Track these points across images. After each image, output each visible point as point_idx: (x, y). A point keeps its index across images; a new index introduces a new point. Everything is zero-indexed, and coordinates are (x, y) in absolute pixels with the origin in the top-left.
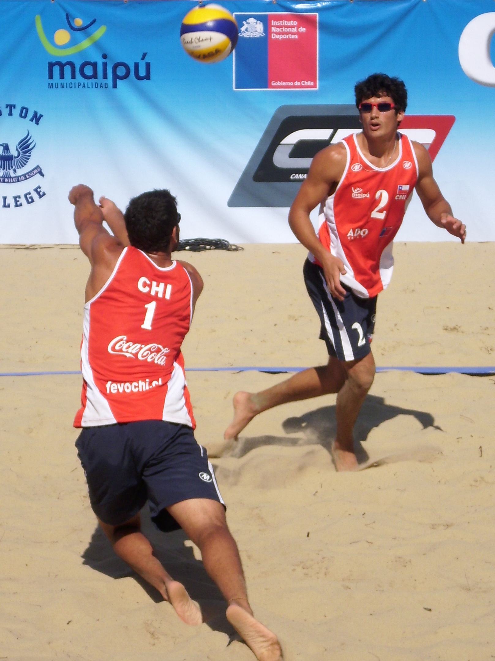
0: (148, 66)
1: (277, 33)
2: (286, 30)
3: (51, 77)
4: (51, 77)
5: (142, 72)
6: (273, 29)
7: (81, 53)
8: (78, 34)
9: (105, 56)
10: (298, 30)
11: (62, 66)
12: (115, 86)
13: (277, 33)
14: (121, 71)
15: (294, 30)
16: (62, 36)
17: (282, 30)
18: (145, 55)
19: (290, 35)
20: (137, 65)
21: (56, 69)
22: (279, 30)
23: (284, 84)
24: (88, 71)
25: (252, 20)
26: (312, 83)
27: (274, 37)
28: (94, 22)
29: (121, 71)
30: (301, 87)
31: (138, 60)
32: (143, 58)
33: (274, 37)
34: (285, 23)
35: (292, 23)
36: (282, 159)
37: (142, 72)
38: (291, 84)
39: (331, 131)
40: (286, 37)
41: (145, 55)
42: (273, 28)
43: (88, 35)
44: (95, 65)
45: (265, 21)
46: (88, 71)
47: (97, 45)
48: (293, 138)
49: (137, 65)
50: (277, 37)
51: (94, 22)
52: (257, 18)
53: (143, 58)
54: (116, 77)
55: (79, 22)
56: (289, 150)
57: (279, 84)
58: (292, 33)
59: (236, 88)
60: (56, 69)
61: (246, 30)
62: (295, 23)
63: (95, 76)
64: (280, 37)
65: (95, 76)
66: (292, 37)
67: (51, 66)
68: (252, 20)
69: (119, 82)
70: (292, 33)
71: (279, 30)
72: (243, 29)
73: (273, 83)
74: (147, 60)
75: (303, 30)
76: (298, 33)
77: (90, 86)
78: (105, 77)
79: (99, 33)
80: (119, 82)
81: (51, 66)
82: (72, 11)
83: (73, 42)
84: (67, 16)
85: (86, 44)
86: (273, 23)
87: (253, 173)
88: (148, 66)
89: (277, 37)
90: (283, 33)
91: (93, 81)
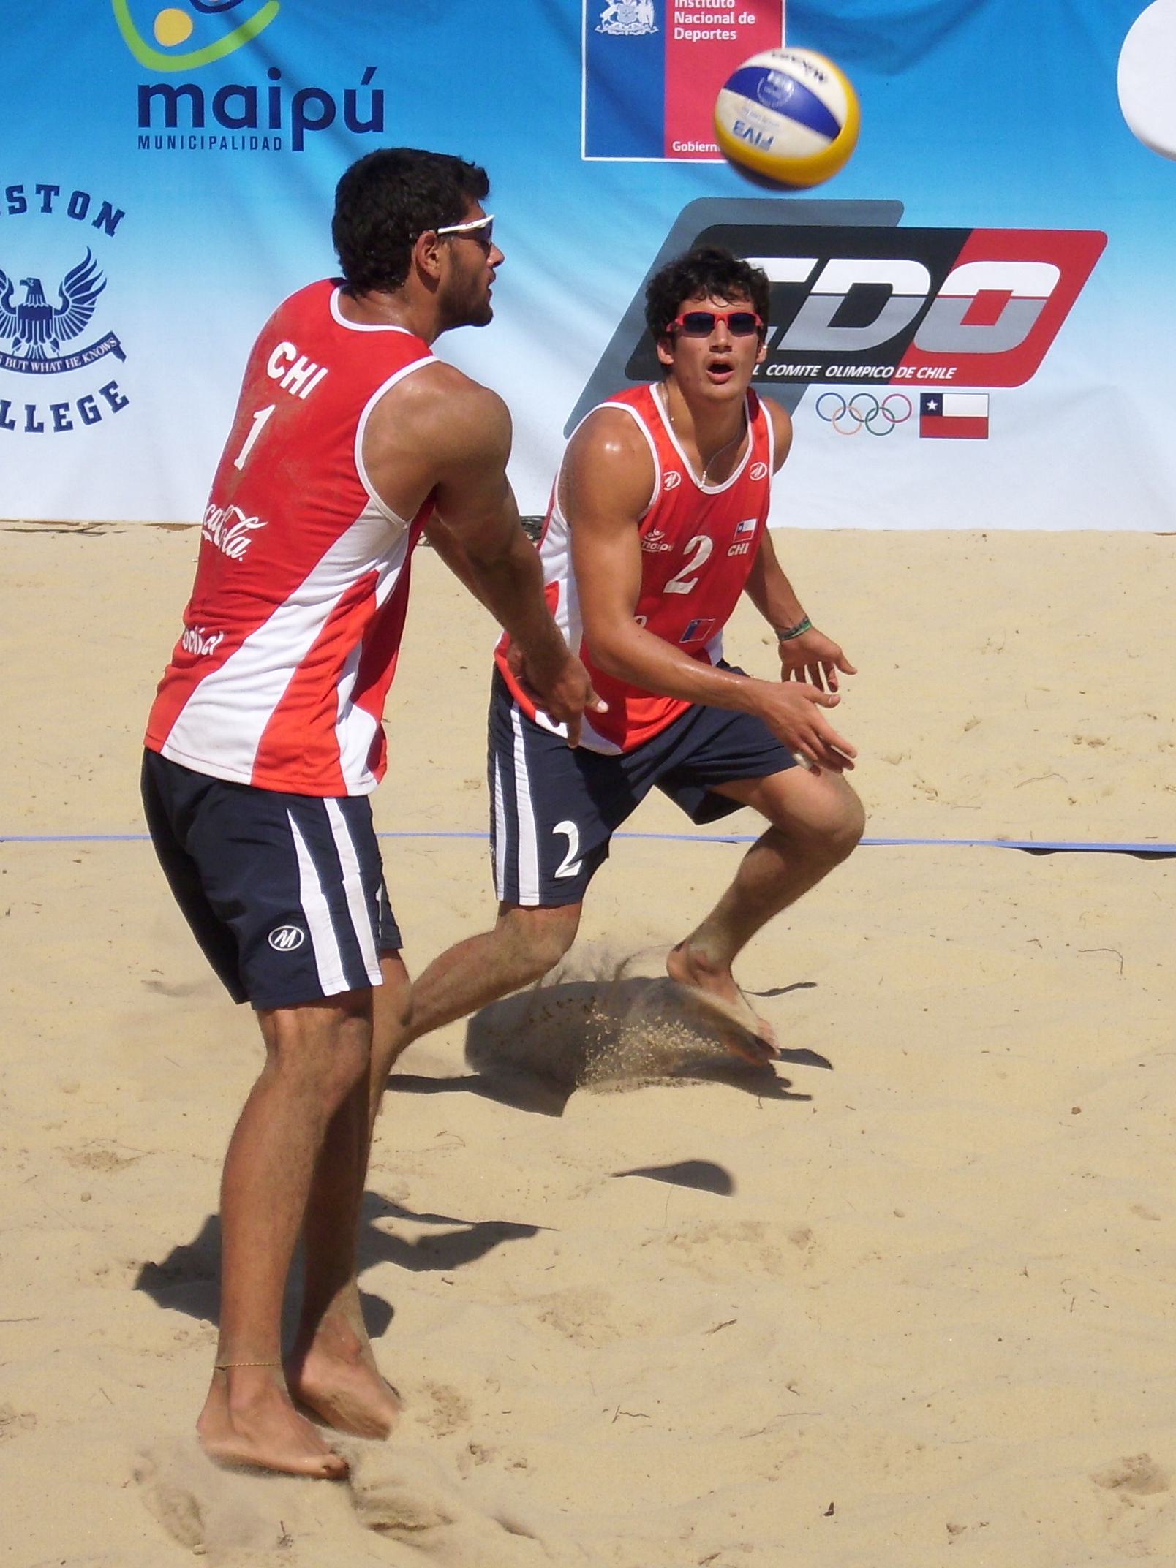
0: (378, 97)
1: (686, 27)
3: (145, 120)
4: (145, 120)
7: (219, 65)
9: (275, 73)
10: (736, 18)
11: (171, 95)
12: (298, 145)
13: (686, 27)
14: (314, 110)
15: (728, 19)
16: (174, 25)
17: (699, 19)
18: (370, 72)
19: (718, 32)
20: (351, 96)
21: (158, 102)
22: (691, 19)
24: (236, 107)
27: (680, 34)
29: (314, 110)
31: (355, 84)
32: (366, 81)
33: (680, 34)
40: (708, 35)
41: (370, 72)
42: (677, 14)
43: (236, 23)
44: (250, 94)
46: (236, 107)
47: (256, 45)
49: (351, 96)
53: (366, 81)
54: (301, 123)
57: (690, 147)
59: (587, 155)
60: (158, 102)
61: (614, 17)
63: (250, 120)
64: (696, 36)
65: (250, 120)
66: (725, 35)
67: (146, 94)
71: (691, 19)
72: (606, 15)
73: (678, 146)
74: (376, 83)
76: (735, 26)
77: (239, 143)
78: (275, 122)
81: (146, 94)
83: (198, 40)
85: (229, 44)
88: (378, 97)
91: (245, 131)
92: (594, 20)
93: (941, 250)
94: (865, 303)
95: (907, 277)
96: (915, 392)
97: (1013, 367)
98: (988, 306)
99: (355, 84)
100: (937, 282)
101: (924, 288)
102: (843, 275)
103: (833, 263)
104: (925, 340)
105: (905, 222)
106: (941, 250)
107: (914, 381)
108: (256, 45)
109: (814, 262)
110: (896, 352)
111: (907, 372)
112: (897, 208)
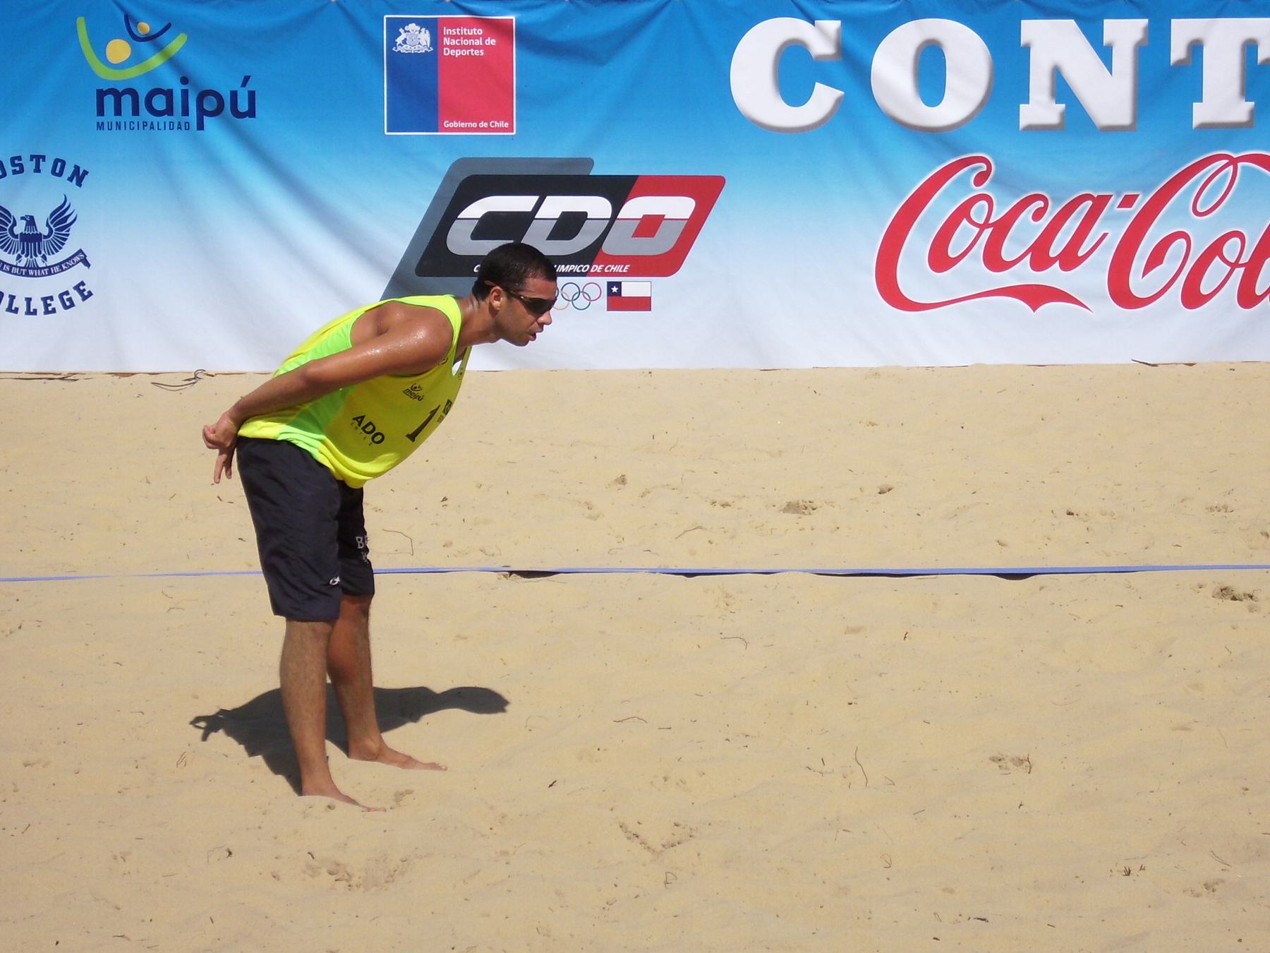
0: (252, 95)
1: (451, 47)
2: (465, 42)
3: (101, 112)
4: (101, 112)
5: (243, 106)
6: (446, 41)
7: (150, 75)
8: (144, 46)
9: (184, 80)
11: (117, 95)
12: (201, 126)
13: (451, 47)
14: (210, 104)
15: (478, 42)
16: (119, 50)
18: (246, 79)
20: (234, 95)
21: (109, 101)
22: (454, 42)
23: (462, 125)
24: (159, 103)
25: (412, 27)
26: (506, 125)
28: (169, 26)
29: (210, 104)
30: (489, 129)
31: (237, 86)
32: (244, 85)
33: (447, 52)
34: (465, 31)
35: (474, 31)
36: (461, 241)
37: (243, 106)
38: (474, 125)
39: (534, 199)
40: (465, 53)
41: (246, 79)
43: (160, 48)
44: (169, 94)
45: (434, 28)
46: (159, 103)
47: (173, 62)
48: (476, 210)
49: (234, 95)
50: (452, 52)
51: (169, 26)
52: (421, 23)
53: (244, 85)
54: (202, 112)
55: (145, 27)
56: (471, 227)
57: (455, 124)
58: (475, 47)
60: (109, 101)
61: (405, 41)
62: (480, 32)
63: (169, 111)
64: (457, 53)
65: (169, 111)
66: (476, 52)
67: (101, 94)
68: (412, 27)
69: (206, 119)
70: (475, 47)
71: (454, 42)
72: (399, 40)
73: (447, 124)
74: (250, 87)
75: (491, 42)
76: (484, 47)
77: (162, 126)
78: (185, 112)
79: (176, 44)
80: (206, 119)
81: (101, 94)
82: (135, 11)
83: (136, 58)
84: (127, 17)
85: (155, 61)
86: (447, 31)
87: (415, 263)
88: (252, 95)
89: (452, 52)
90: (461, 47)
91: (166, 118)
92: (392, 43)
93: (617, 190)
94: (570, 224)
95: (597, 207)
96: (603, 281)
97: (667, 264)
98: (650, 225)
99: (237, 86)
100: (616, 209)
101: (608, 215)
102: (555, 206)
103: (549, 200)
104: (608, 248)
105: (596, 171)
106: (617, 190)
107: (602, 274)
108: (173, 62)
109: (536, 198)
110: (591, 255)
111: (598, 268)
112: (590, 163)
